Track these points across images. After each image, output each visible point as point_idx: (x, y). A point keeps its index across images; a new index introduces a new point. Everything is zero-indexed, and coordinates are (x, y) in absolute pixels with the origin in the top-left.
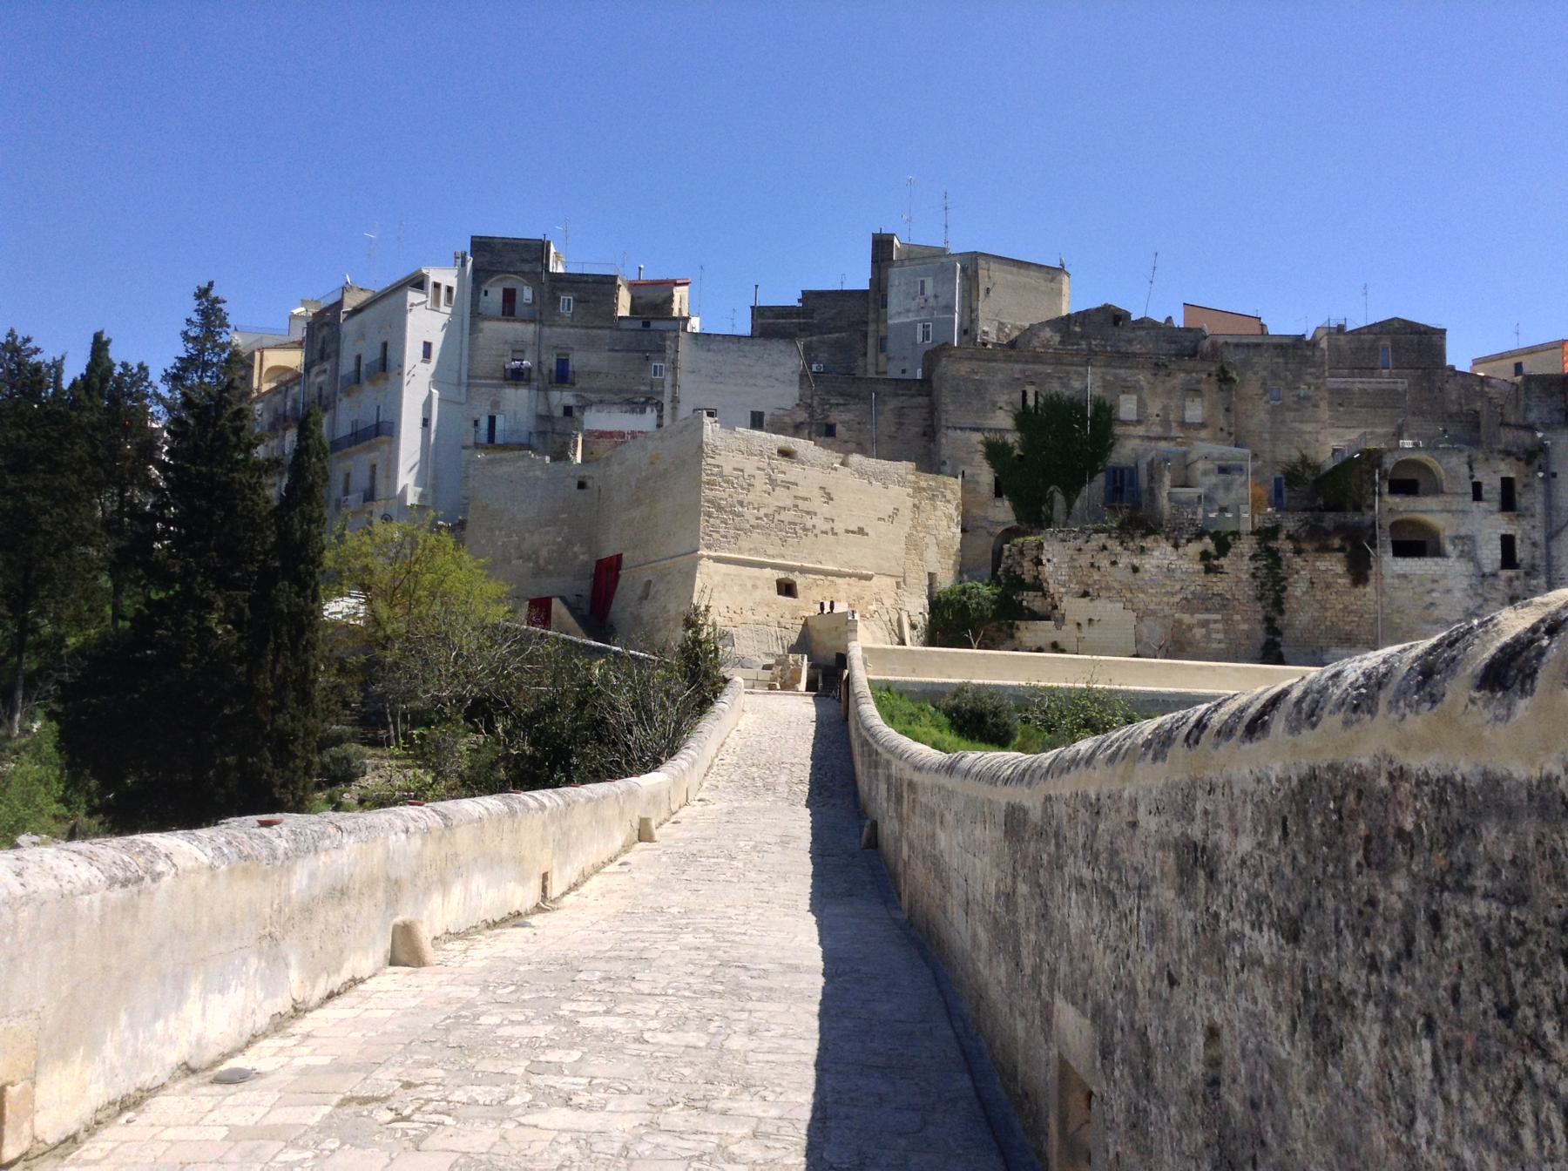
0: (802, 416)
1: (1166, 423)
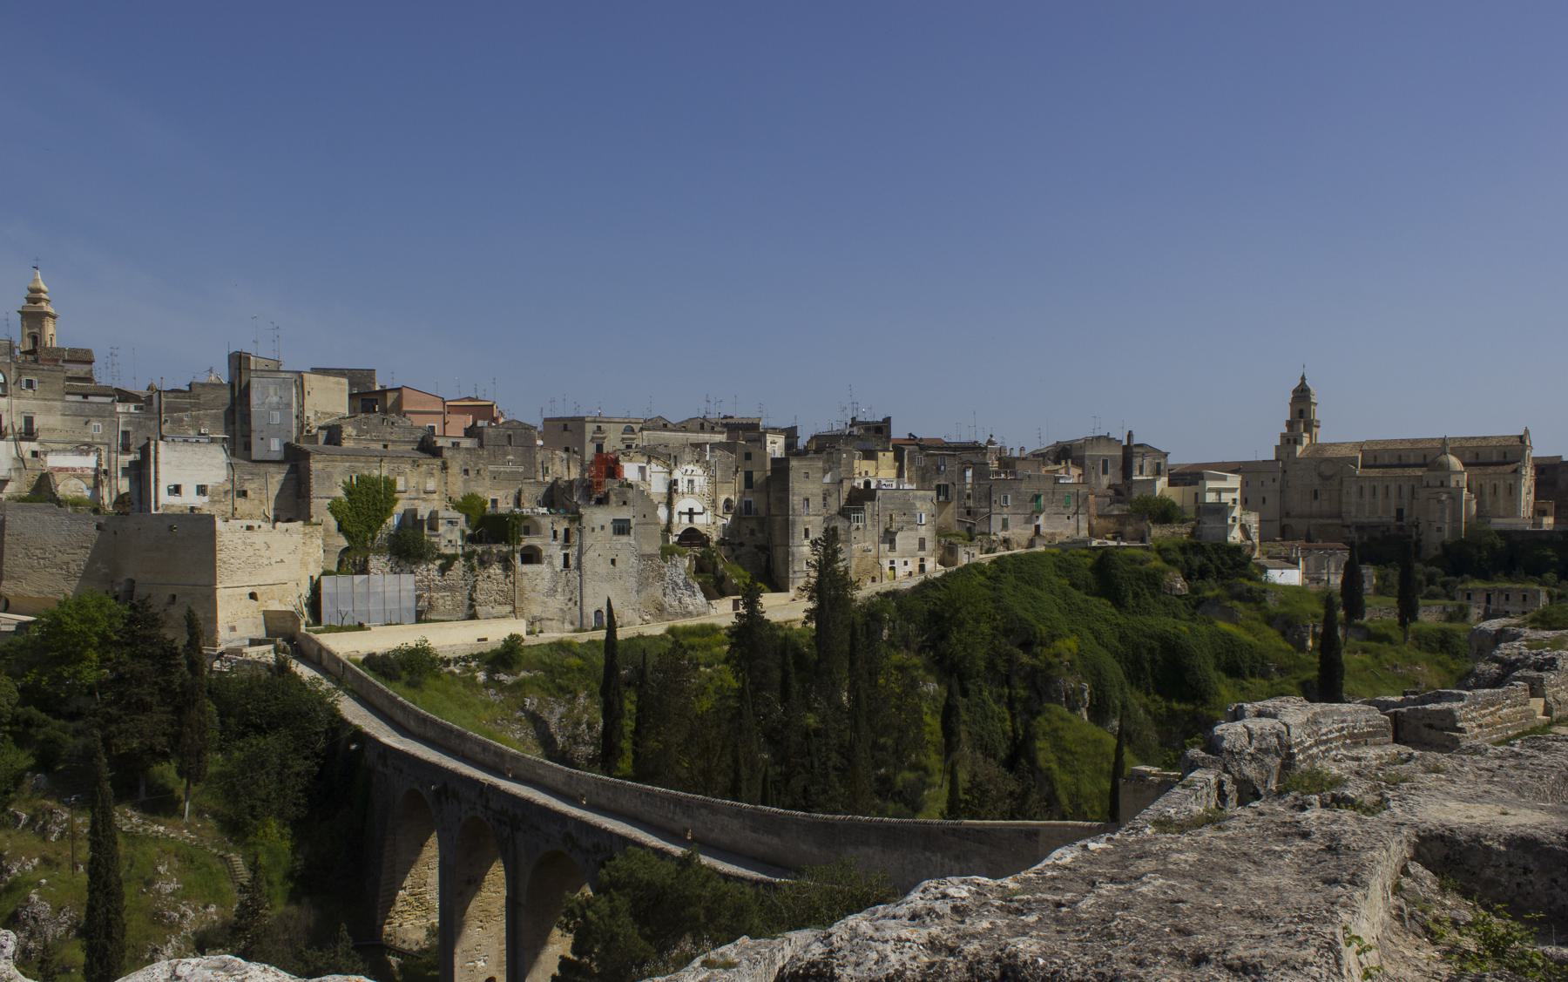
0: (229, 486)
1: (418, 491)
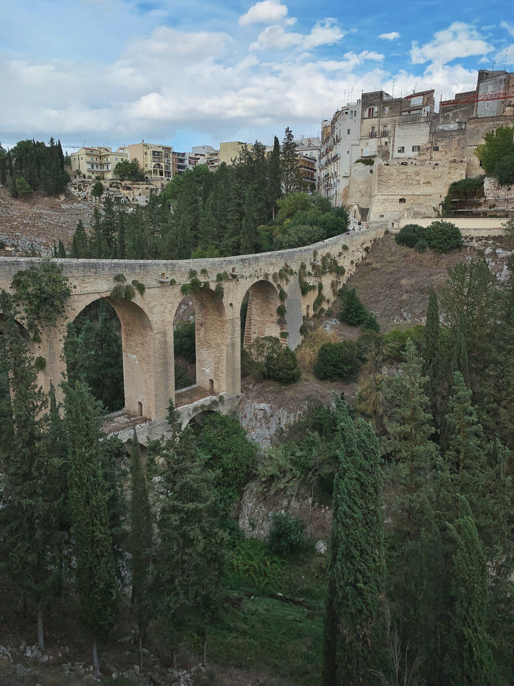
0: (429, 145)
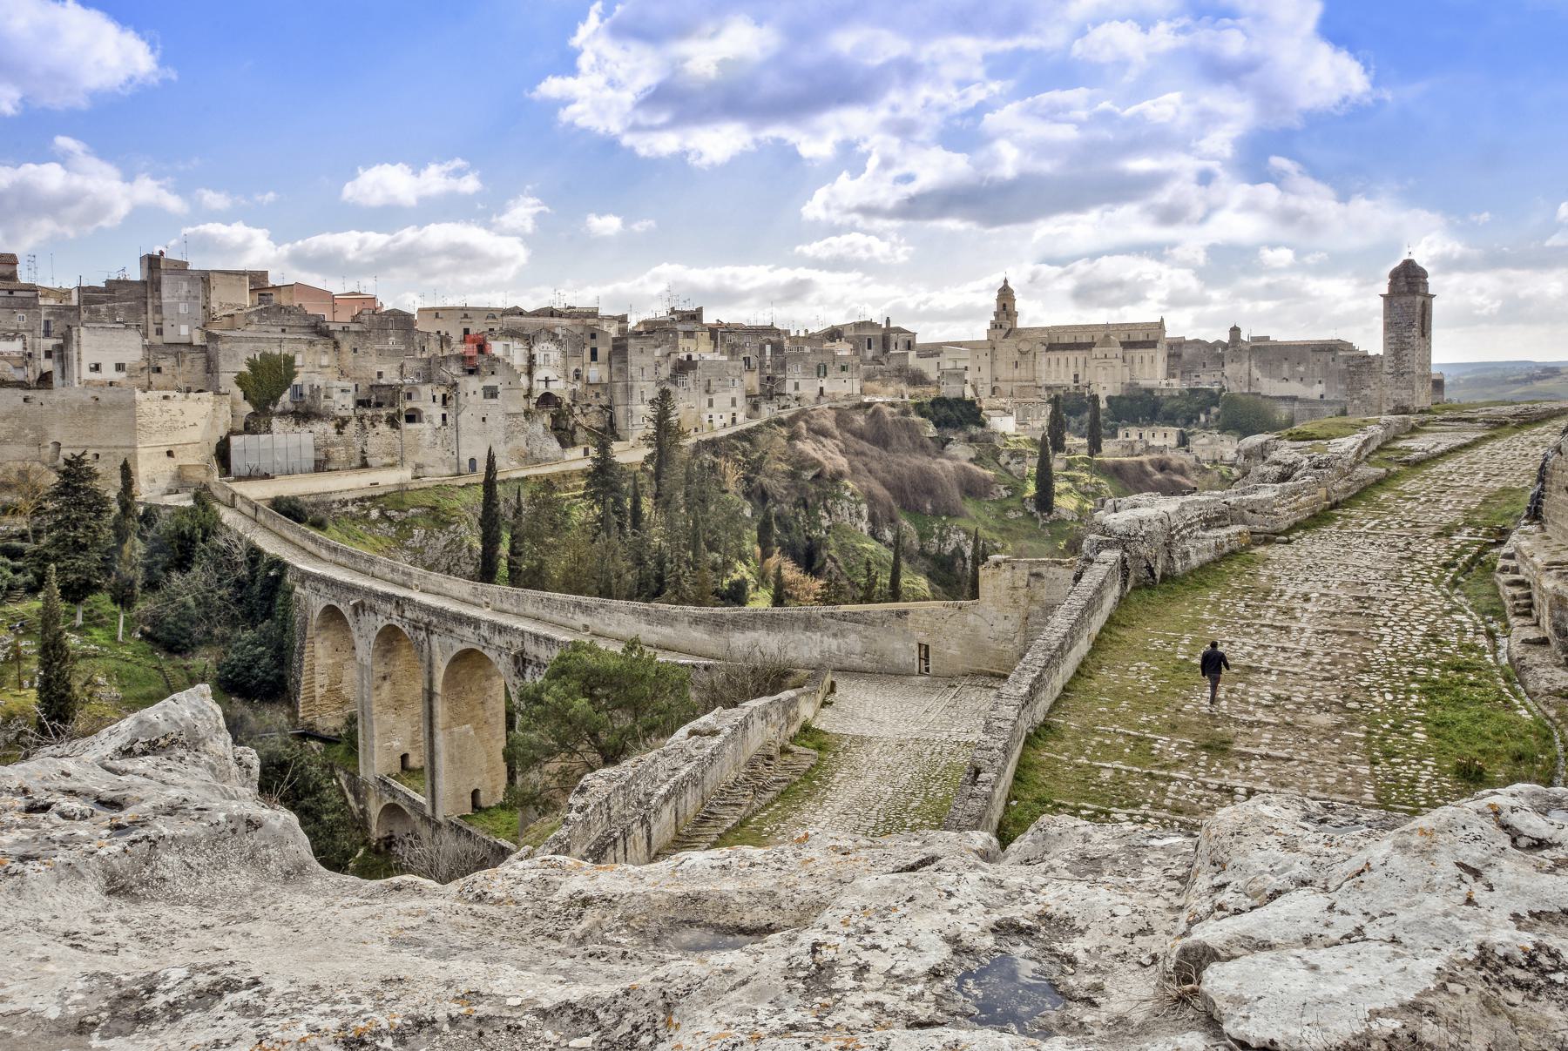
0: (145, 364)
